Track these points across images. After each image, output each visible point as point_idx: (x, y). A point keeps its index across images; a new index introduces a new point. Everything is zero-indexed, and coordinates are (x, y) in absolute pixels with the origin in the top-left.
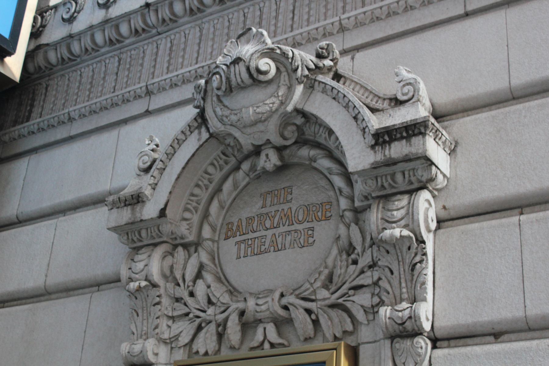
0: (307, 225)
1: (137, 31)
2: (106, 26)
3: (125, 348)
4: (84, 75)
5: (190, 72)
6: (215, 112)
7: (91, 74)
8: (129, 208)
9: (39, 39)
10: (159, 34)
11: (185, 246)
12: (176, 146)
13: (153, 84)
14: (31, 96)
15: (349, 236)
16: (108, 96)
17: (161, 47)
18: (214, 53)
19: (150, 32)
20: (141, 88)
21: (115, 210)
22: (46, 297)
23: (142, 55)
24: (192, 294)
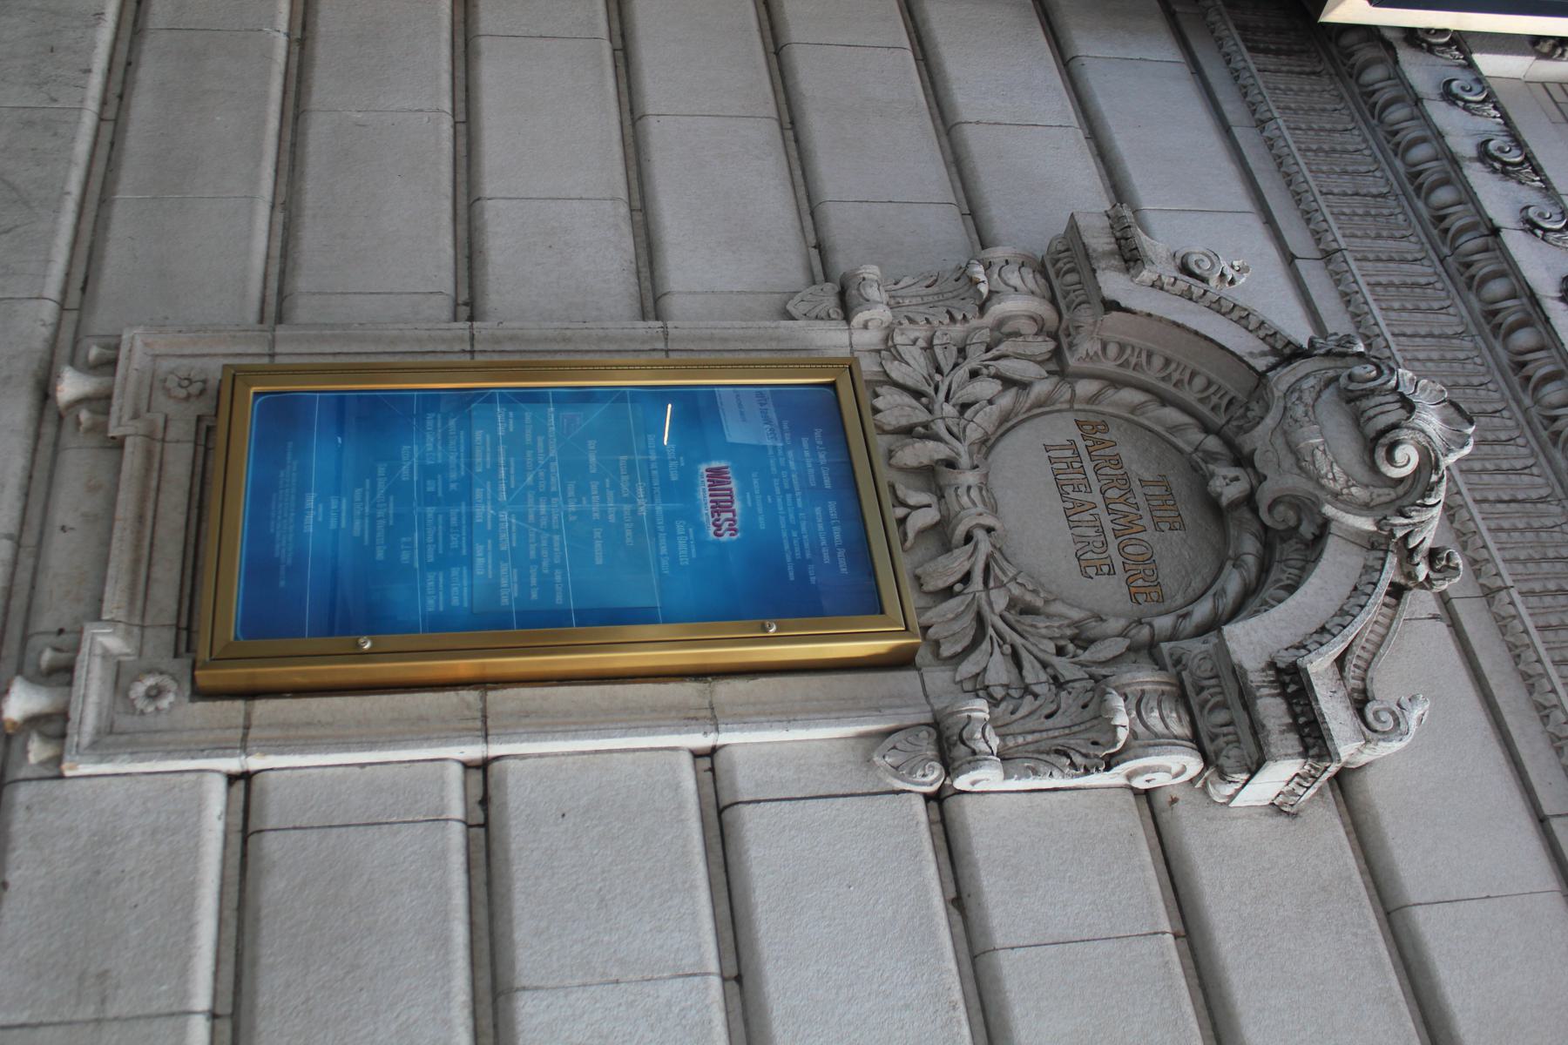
0: (1118, 561)
1: (1443, 218)
2: (1445, 162)
3: (871, 271)
4: (1347, 136)
5: (1376, 324)
6: (1307, 376)
7: (1351, 148)
8: (1114, 247)
9: (1404, 45)
10: (1442, 261)
11: (1057, 354)
12: (1235, 315)
13: (1345, 261)
14: (1296, 48)
15: (1105, 637)
16: (1312, 184)
17: (1417, 268)
18: (1416, 364)
19: (1444, 243)
20: (1335, 240)
21: (1107, 222)
22: (941, 127)
23: (1397, 234)
24: (974, 374)
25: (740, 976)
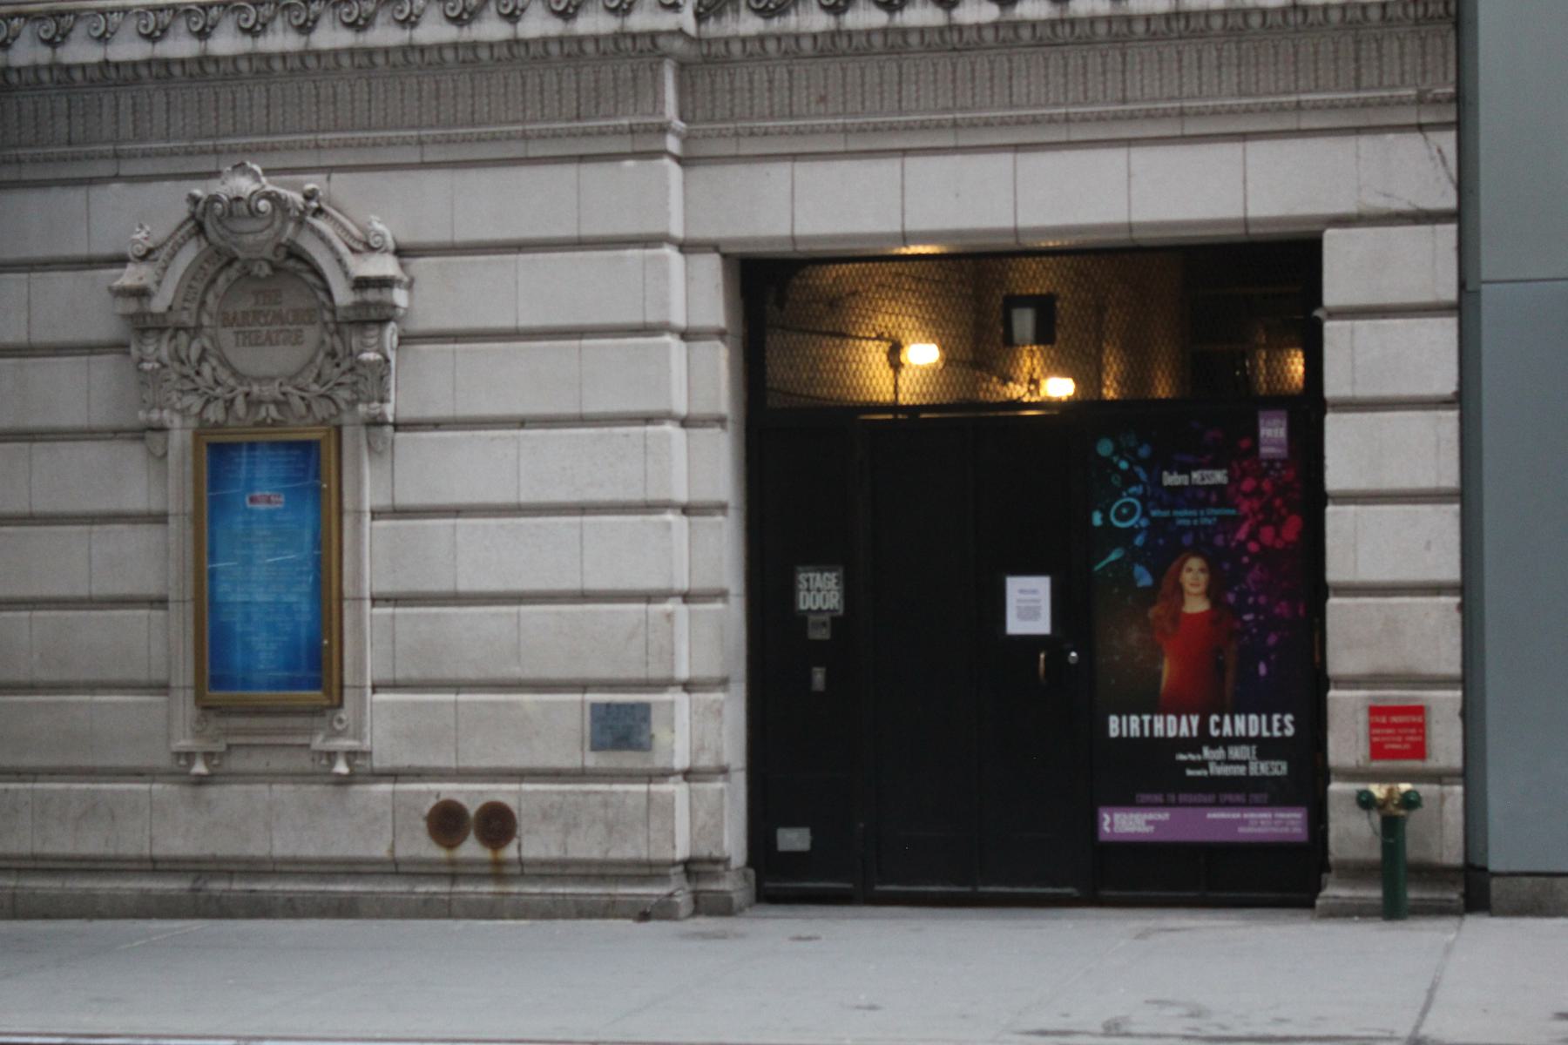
0: (294, 327)
3: (142, 415)
11: (186, 329)
24: (198, 373)
25: (457, 512)
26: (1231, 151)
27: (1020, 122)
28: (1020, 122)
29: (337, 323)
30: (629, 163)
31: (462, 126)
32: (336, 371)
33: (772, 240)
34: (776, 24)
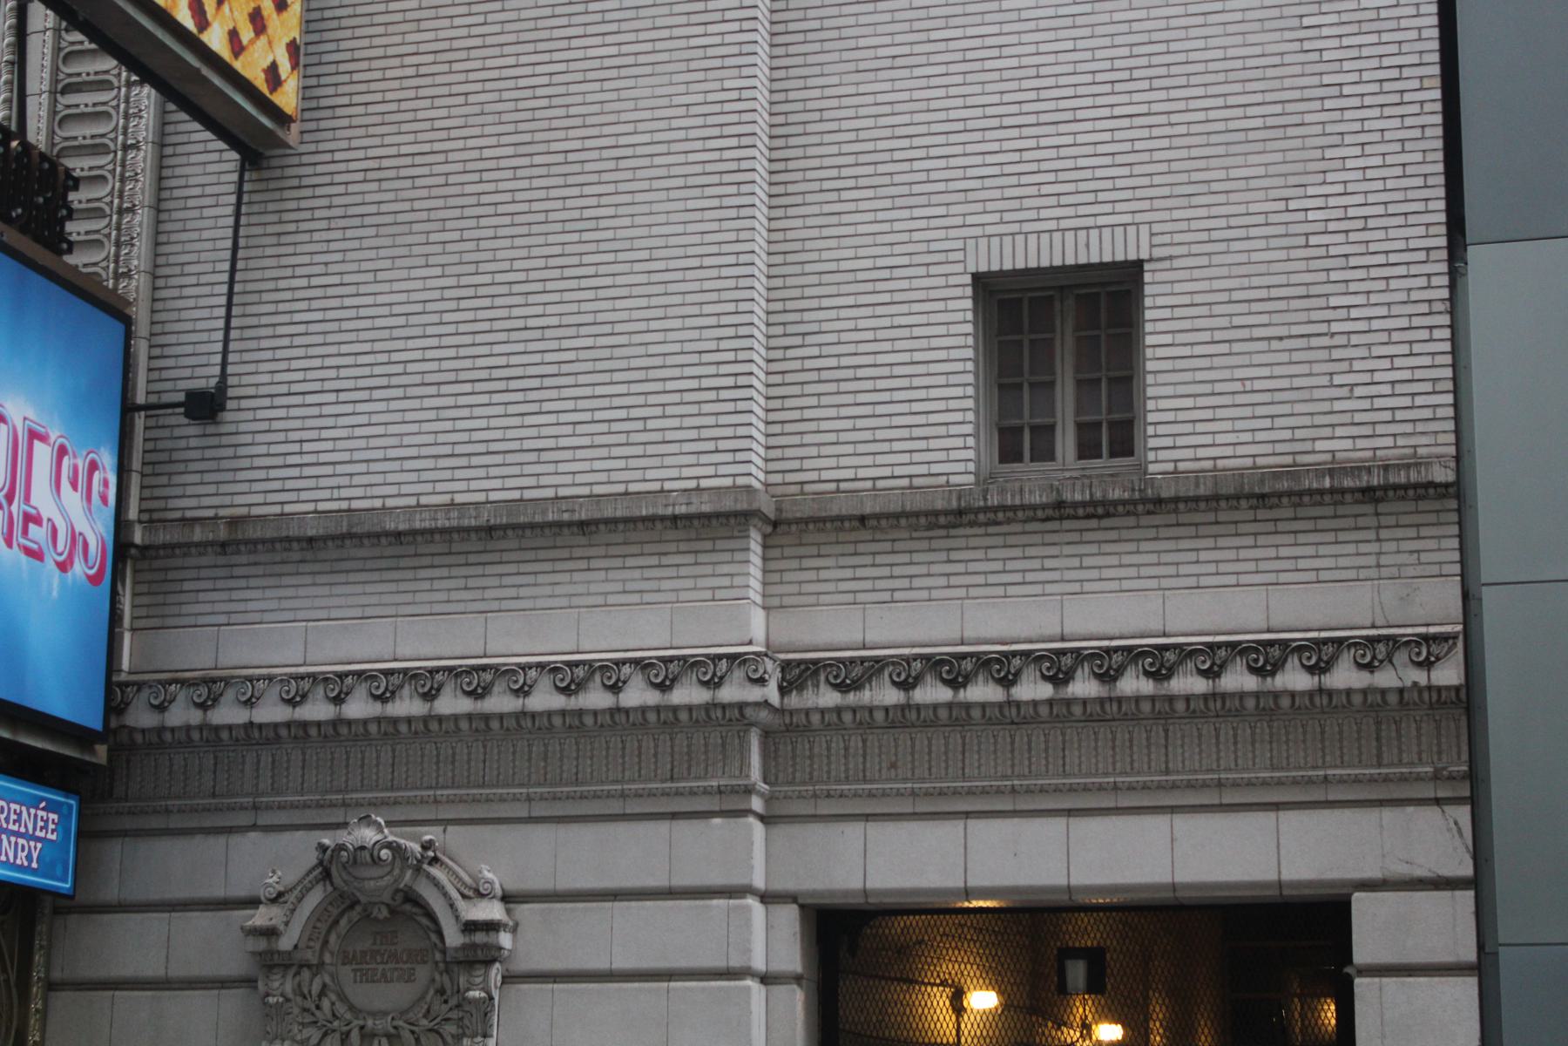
11: (309, 966)
24: (318, 1007)
26: (1266, 819)
27: (1072, 789)
28: (1072, 789)
29: (445, 962)
30: (717, 821)
31: (566, 785)
32: (445, 1007)
33: (846, 893)
34: (852, 698)
